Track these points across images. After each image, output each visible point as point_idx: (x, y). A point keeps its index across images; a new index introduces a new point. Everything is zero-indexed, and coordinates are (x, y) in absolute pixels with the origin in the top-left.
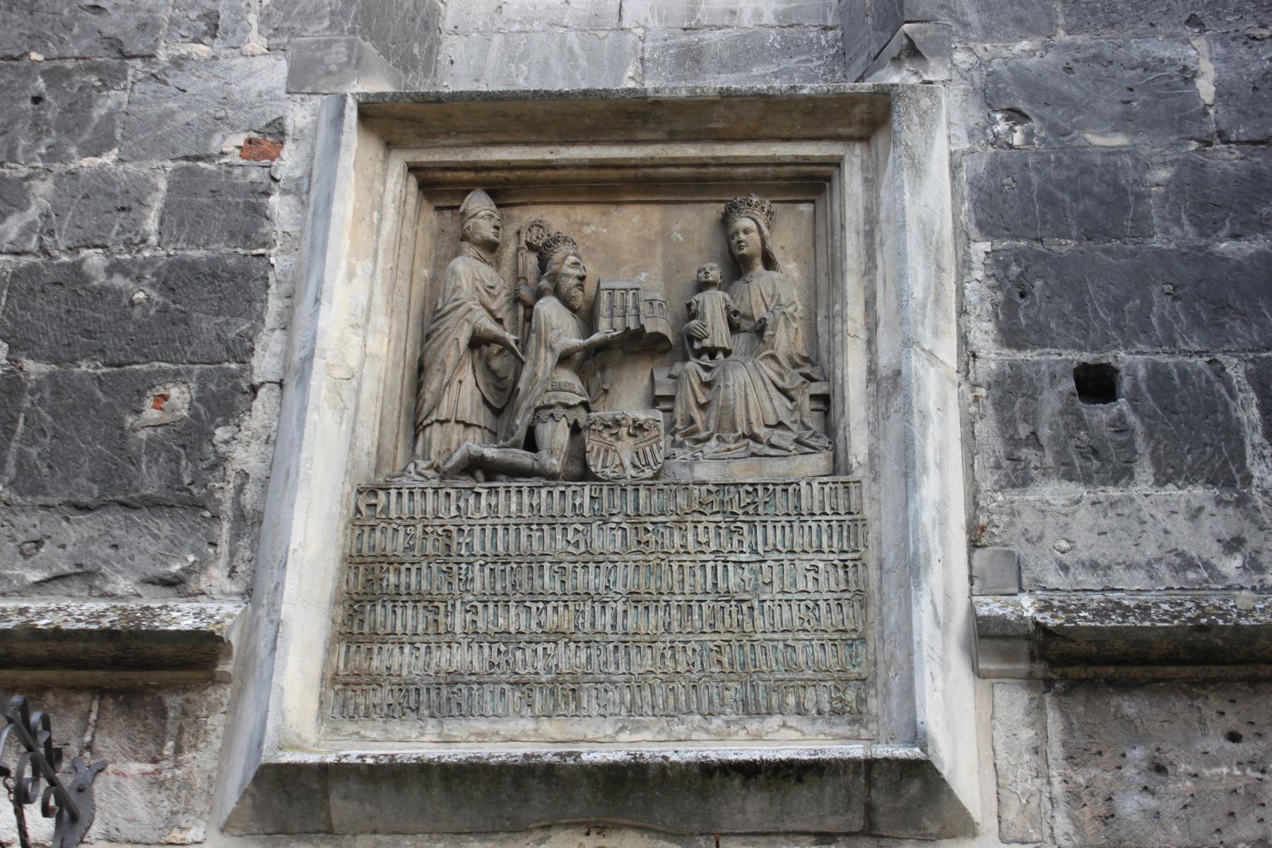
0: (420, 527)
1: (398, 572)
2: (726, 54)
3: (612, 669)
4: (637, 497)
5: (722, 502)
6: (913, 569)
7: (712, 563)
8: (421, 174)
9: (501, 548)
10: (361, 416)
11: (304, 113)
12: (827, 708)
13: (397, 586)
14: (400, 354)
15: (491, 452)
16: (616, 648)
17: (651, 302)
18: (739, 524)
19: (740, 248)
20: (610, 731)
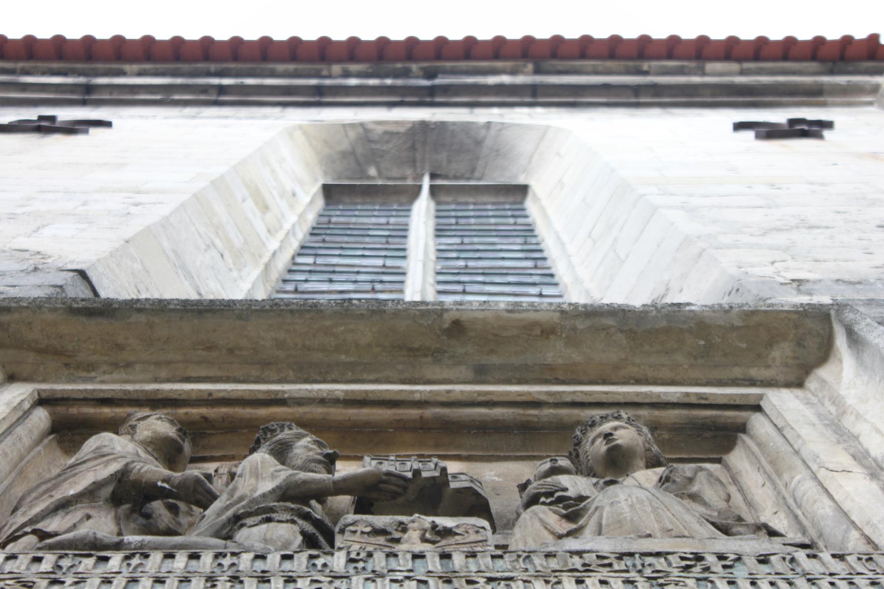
8: (60, 409)
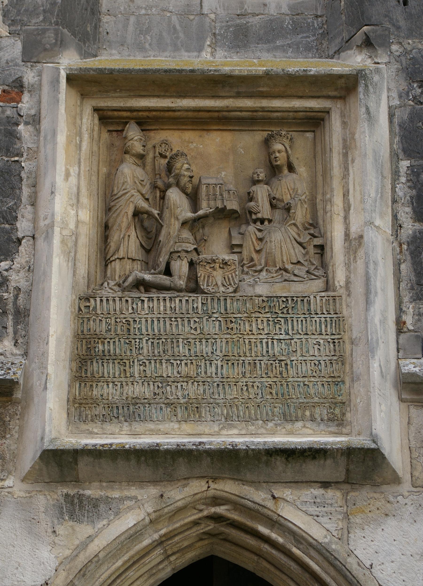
0: (113, 318)
1: (103, 343)
2: (262, 32)
3: (217, 397)
4: (226, 304)
5: (270, 307)
6: (371, 350)
7: (266, 340)
9: (156, 331)
10: (78, 256)
11: (33, 74)
12: (326, 418)
13: (103, 351)
14: (95, 219)
15: (148, 277)
16: (218, 385)
17: (229, 191)
18: (279, 319)
19: (276, 161)
20: (217, 429)
